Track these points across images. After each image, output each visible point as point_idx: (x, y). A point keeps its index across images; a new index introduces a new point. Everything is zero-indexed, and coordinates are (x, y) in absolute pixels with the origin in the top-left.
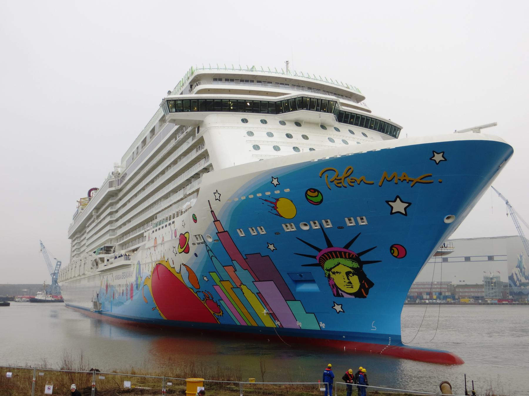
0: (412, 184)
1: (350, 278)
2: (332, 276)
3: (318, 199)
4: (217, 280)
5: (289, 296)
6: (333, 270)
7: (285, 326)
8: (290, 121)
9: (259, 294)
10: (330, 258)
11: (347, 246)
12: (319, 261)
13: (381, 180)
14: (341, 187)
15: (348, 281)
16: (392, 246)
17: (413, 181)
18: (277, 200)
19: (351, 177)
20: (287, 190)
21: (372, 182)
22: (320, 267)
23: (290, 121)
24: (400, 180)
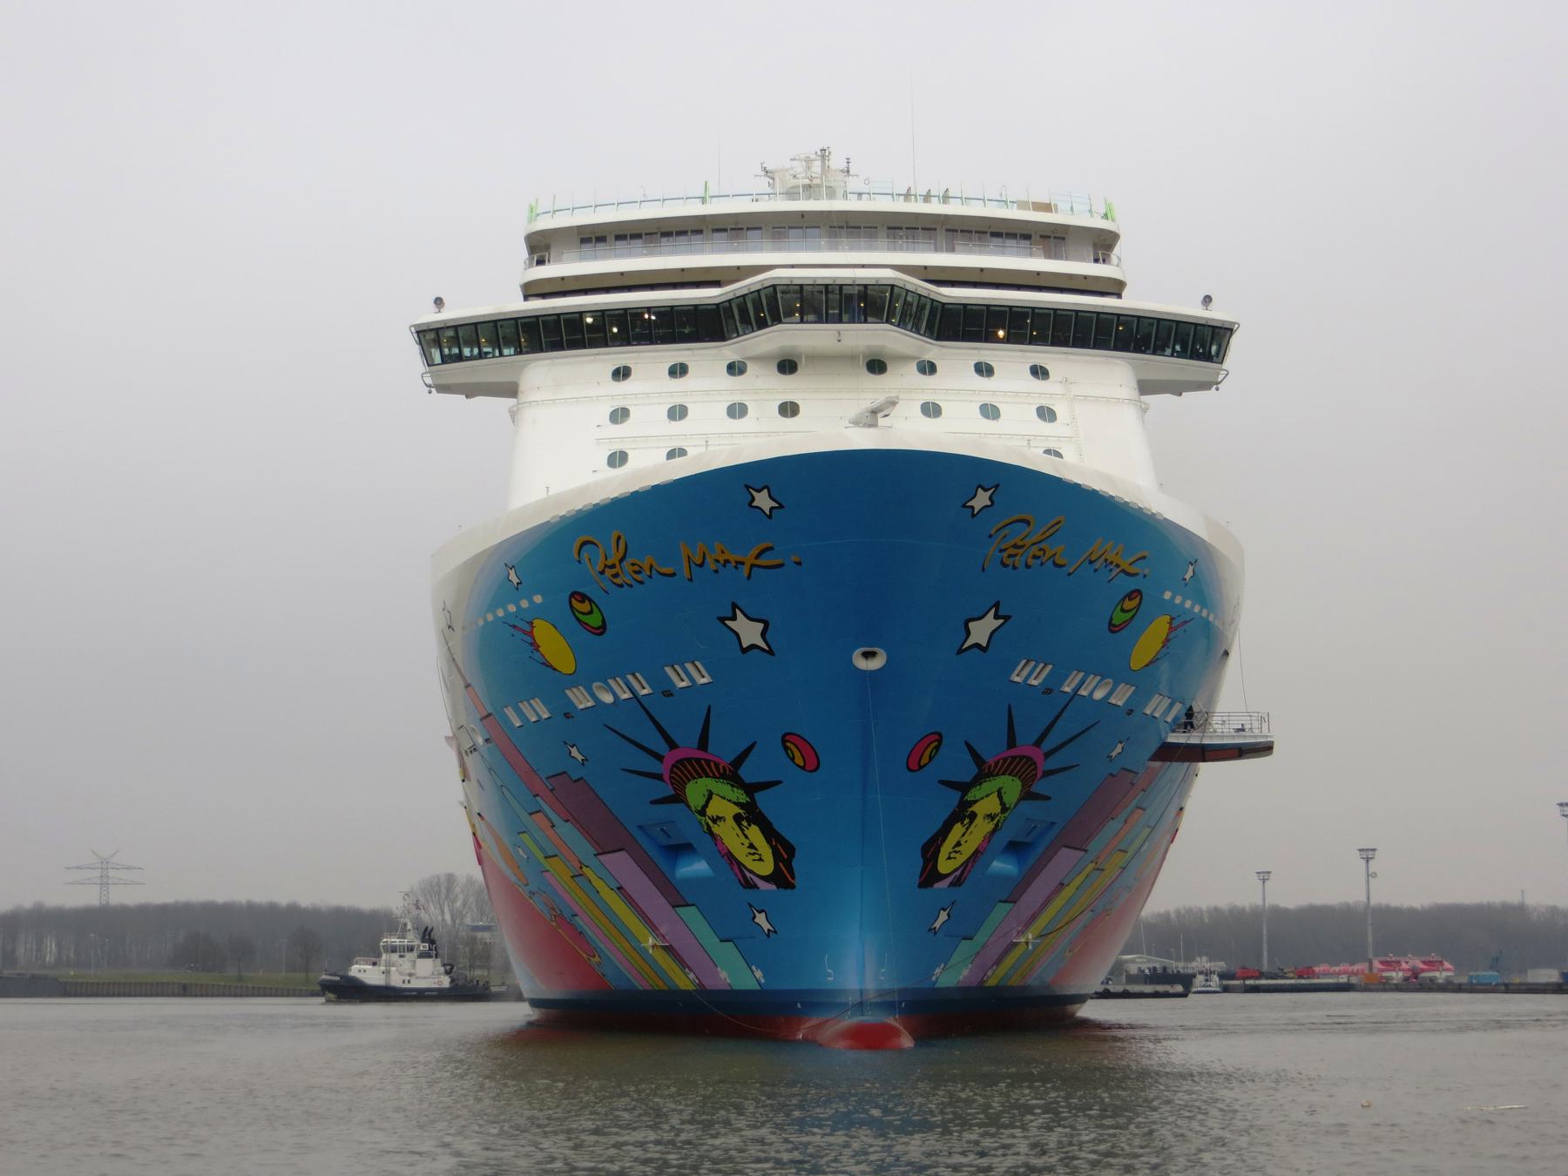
2: (715, 829)
3: (594, 620)
4: (540, 856)
5: (676, 897)
6: (710, 811)
7: (710, 984)
8: (761, 359)
9: (620, 888)
14: (621, 586)
16: (784, 741)
18: (531, 623)
19: (629, 560)
20: (538, 599)
21: (669, 570)
22: (682, 806)
23: (761, 359)
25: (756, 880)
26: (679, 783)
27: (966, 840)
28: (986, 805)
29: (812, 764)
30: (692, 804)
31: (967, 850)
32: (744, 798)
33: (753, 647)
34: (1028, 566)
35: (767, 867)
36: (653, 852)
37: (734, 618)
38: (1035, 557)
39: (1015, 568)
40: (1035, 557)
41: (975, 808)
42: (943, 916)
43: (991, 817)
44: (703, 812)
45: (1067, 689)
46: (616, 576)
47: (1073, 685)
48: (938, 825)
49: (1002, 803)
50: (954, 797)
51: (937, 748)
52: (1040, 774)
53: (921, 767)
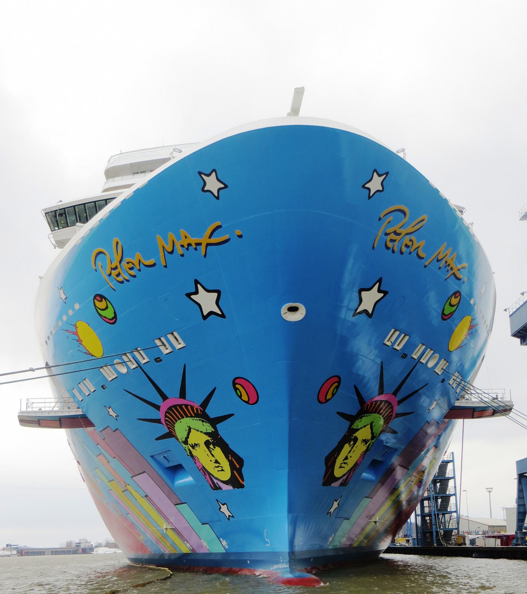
0: (202, 248)
1: (213, 452)
2: (194, 452)
6: (191, 441)
10: (176, 421)
11: (183, 394)
12: (169, 428)
13: (162, 254)
15: (213, 460)
16: (234, 384)
17: (200, 244)
24: (182, 246)
25: (221, 484)
26: (171, 424)
27: (351, 455)
28: (364, 434)
29: (253, 399)
30: (179, 437)
31: (351, 463)
32: (210, 429)
33: (211, 313)
34: (402, 253)
35: (226, 475)
36: (160, 472)
37: (196, 292)
38: (407, 246)
39: (393, 252)
40: (407, 246)
41: (357, 434)
42: (336, 505)
43: (365, 441)
44: (186, 442)
45: (415, 357)
46: (118, 275)
47: (418, 354)
48: (336, 444)
49: (372, 433)
50: (347, 423)
51: (337, 387)
52: (394, 415)
53: (327, 401)
